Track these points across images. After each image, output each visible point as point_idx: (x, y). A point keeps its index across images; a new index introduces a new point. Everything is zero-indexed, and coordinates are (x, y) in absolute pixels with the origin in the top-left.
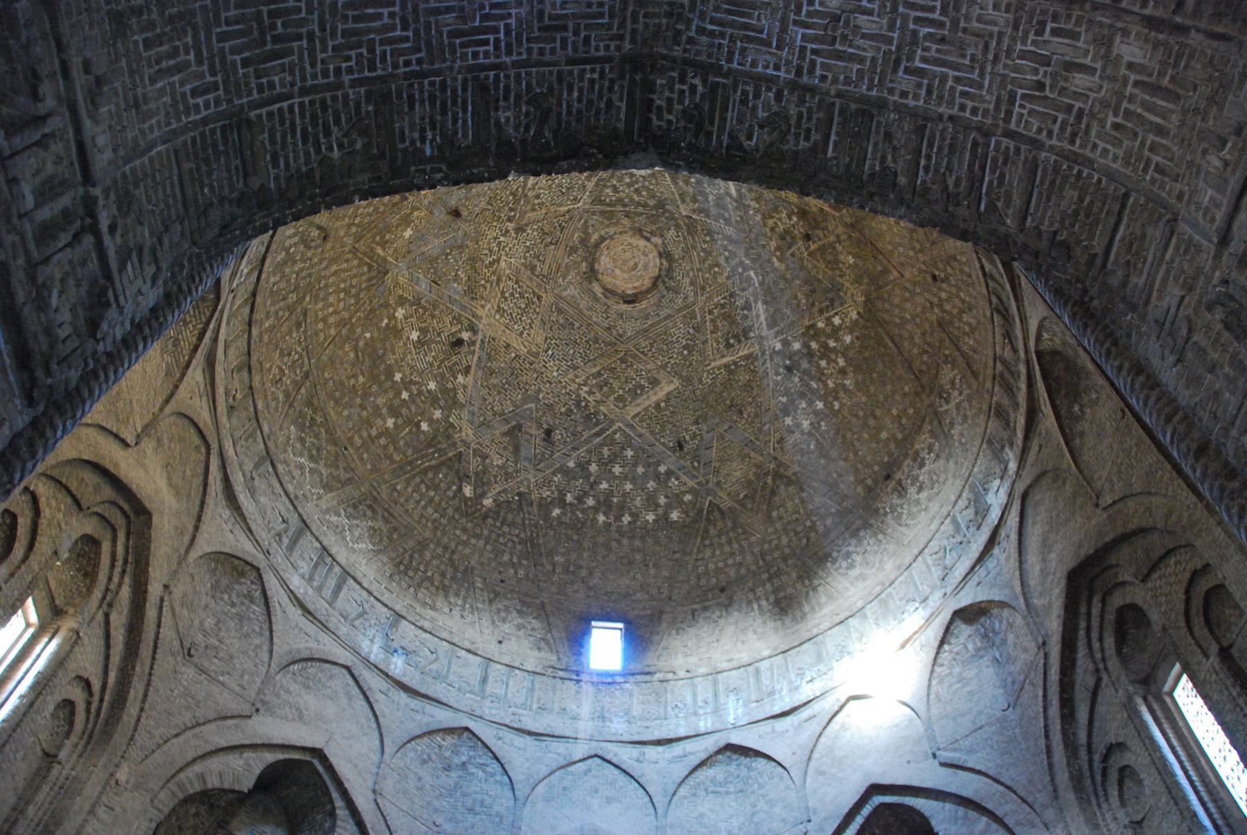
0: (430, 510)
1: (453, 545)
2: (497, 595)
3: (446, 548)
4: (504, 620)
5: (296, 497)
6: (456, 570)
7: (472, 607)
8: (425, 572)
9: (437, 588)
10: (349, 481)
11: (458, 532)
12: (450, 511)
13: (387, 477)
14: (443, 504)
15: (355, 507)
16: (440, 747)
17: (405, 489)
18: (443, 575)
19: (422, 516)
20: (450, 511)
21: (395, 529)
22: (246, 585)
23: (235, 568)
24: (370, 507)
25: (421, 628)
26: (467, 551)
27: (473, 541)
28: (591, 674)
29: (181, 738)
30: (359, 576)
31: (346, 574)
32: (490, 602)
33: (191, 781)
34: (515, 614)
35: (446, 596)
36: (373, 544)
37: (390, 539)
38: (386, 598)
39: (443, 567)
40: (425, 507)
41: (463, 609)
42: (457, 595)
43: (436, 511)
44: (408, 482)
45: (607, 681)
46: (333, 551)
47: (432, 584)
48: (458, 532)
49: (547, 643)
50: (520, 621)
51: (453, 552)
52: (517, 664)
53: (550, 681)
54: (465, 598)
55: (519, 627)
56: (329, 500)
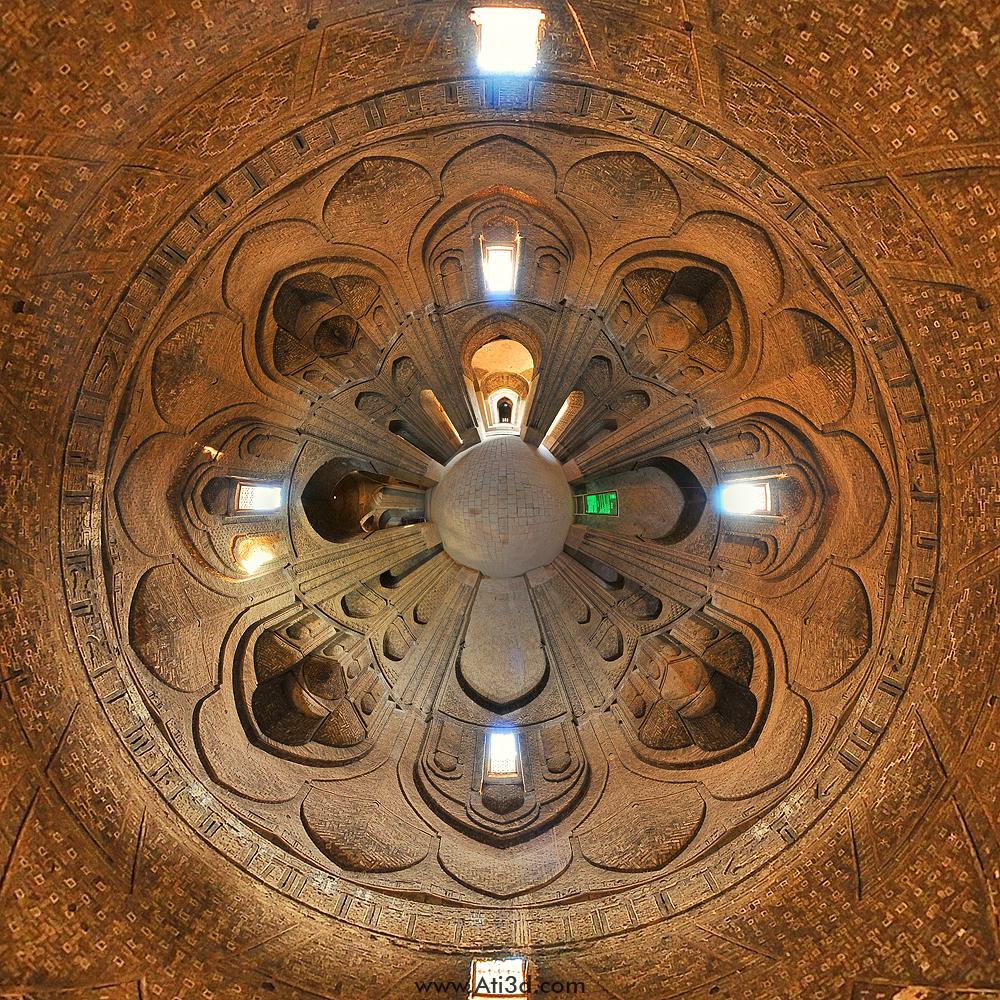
0: (901, 908)
1: (828, 942)
2: (710, 971)
3: (831, 929)
4: (677, 957)
5: (923, 660)
6: (792, 935)
7: (734, 935)
8: (820, 888)
9: (789, 900)
10: (955, 732)
11: (842, 957)
12: (885, 949)
13: (971, 805)
14: (904, 937)
15: (926, 762)
16: (668, 837)
17: (950, 854)
18: (799, 914)
19: (898, 891)
20: (885, 949)
21: (892, 841)
22: (850, 645)
23: (859, 624)
24: (927, 788)
25: (765, 865)
26: (802, 964)
27: (808, 979)
28: (520, 955)
29: (774, 633)
30: (855, 787)
31: (856, 769)
32: (713, 959)
33: (757, 647)
34: (666, 973)
35: (772, 908)
36: (881, 806)
37: (882, 833)
38: (819, 826)
39: (810, 915)
40: (911, 897)
41: (740, 924)
42: (762, 924)
43: (895, 921)
44: (961, 856)
45: (497, 952)
46: (883, 746)
47: (799, 894)
48: (842, 957)
49: (596, 969)
50: (654, 971)
51: (816, 941)
52: (631, 935)
53: (576, 936)
54: (748, 931)
55: (650, 964)
56: (930, 711)
